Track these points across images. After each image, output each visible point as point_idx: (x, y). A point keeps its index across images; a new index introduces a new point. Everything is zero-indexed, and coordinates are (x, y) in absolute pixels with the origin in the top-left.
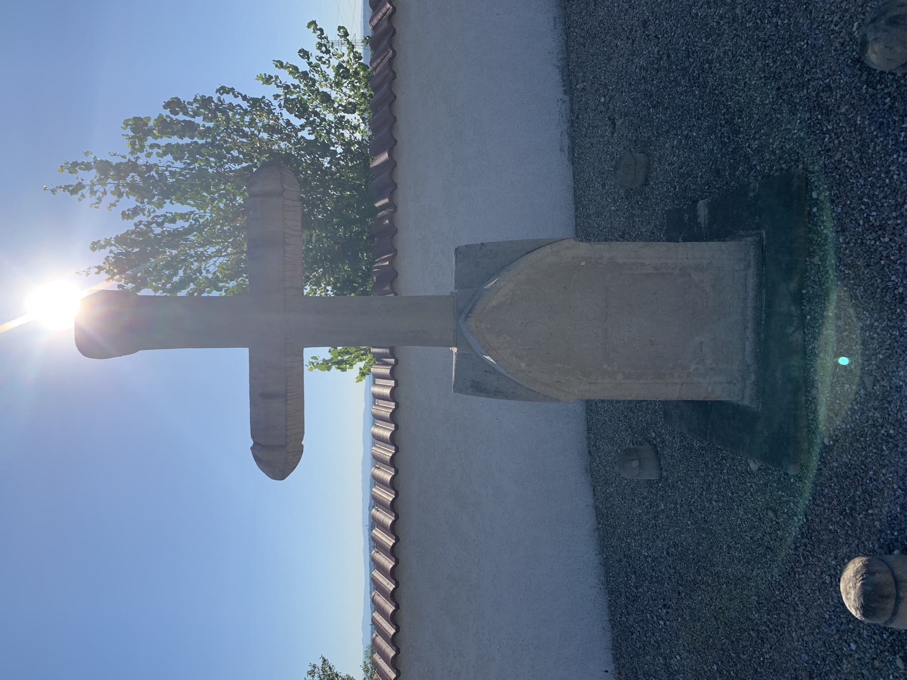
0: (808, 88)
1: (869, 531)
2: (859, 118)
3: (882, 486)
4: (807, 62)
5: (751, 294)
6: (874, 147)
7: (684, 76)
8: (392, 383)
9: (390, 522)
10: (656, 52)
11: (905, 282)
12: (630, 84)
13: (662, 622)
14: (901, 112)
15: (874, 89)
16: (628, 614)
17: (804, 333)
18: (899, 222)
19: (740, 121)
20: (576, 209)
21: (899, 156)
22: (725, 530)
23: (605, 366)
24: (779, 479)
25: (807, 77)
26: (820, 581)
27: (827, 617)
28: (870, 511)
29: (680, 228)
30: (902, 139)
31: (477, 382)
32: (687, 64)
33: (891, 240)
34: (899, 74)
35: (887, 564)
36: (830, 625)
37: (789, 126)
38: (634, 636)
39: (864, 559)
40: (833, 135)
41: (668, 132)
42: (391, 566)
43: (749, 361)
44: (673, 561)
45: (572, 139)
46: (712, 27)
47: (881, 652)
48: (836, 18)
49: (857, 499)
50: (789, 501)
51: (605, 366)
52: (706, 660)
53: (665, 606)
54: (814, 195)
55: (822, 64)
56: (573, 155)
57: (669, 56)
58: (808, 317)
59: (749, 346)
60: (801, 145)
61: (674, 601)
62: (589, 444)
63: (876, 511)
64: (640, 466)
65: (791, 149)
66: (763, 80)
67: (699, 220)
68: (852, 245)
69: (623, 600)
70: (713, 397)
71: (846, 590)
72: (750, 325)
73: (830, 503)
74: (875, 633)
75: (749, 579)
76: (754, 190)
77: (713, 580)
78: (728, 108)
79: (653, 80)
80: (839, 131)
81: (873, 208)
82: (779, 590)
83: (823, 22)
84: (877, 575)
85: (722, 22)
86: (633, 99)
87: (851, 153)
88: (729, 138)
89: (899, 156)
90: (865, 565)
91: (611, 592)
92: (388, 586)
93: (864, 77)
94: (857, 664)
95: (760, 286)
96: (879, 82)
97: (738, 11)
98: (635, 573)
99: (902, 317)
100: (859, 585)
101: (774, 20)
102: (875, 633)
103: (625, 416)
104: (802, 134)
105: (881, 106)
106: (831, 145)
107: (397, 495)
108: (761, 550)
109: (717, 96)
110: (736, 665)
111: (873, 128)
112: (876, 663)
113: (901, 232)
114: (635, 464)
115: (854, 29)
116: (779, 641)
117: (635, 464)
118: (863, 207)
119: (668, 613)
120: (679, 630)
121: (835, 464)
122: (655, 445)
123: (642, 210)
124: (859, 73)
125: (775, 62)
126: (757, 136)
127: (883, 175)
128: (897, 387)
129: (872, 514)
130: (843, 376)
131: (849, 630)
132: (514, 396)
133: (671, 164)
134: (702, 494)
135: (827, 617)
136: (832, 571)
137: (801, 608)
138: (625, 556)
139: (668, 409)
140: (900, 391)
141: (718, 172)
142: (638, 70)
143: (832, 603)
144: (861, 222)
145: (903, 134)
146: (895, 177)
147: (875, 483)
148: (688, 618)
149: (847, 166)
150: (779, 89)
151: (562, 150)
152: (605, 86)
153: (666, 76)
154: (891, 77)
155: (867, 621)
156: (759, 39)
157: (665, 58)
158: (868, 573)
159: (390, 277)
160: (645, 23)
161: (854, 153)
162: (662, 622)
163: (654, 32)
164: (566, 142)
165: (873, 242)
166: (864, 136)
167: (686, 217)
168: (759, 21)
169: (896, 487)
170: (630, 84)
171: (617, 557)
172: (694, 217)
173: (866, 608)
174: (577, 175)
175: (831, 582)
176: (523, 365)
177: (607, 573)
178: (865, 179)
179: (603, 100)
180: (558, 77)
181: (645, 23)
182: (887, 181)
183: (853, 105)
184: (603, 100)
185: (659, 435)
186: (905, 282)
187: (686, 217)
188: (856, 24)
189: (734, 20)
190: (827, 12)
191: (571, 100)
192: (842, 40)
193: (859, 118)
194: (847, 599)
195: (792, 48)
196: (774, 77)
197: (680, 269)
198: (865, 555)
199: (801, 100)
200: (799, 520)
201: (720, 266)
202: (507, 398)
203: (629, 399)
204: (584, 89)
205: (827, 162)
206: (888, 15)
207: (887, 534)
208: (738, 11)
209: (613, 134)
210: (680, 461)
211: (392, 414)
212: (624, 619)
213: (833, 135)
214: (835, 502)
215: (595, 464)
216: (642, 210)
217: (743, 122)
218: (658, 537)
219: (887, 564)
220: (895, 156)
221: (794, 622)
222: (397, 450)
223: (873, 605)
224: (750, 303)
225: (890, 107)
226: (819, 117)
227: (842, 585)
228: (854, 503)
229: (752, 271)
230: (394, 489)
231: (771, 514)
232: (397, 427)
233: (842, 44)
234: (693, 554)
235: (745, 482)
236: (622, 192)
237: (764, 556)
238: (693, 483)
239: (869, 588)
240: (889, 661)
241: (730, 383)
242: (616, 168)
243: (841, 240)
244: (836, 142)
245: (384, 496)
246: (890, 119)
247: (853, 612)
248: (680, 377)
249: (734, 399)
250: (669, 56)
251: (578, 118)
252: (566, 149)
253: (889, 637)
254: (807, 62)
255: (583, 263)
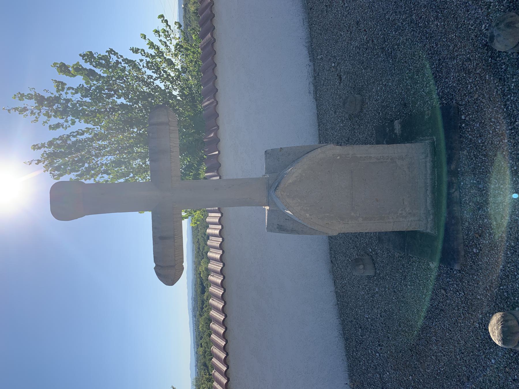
0: (457, 60)
1: (501, 298)
2: (487, 76)
3: (508, 273)
4: (456, 45)
5: (429, 172)
6: (497, 92)
7: (382, 53)
8: (220, 227)
9: (222, 306)
10: (365, 38)
11: (517, 164)
12: (350, 56)
13: (378, 354)
14: (511, 73)
15: (496, 60)
16: (357, 351)
17: (460, 192)
18: (513, 131)
19: (417, 77)
20: (319, 125)
21: (511, 96)
22: (416, 301)
23: (353, 214)
24: (447, 272)
25: (456, 54)
26: (473, 327)
27: (477, 346)
28: (501, 288)
29: (385, 136)
30: (512, 87)
31: (280, 225)
32: (384, 45)
33: (508, 141)
34: (510, 53)
35: (513, 315)
36: (479, 351)
37: (447, 80)
38: (361, 363)
39: (501, 313)
40: (472, 85)
41: (374, 82)
42: (223, 332)
43: (429, 208)
44: (384, 320)
45: (316, 87)
46: (398, 26)
47: (510, 363)
48: (472, 22)
49: (494, 281)
50: (454, 284)
51: (353, 214)
52: (405, 374)
53: (379, 345)
54: (463, 117)
55: (465, 47)
56: (316, 95)
57: (373, 41)
58: (462, 183)
59: (429, 201)
60: (454, 90)
61: (385, 342)
62: (331, 257)
63: (505, 287)
64: (364, 268)
65: (448, 92)
66: (430, 55)
67: (395, 132)
68: (486, 144)
69: (354, 343)
70: (411, 229)
71: (492, 331)
72: (429, 188)
73: (478, 284)
74: (506, 353)
75: (430, 328)
76: (428, 115)
77: (409, 330)
78: (410, 70)
79: (363, 54)
80: (476, 83)
81: (498, 124)
82: (448, 333)
83: (464, 24)
84: (510, 322)
85: (404, 23)
86: (352, 65)
87: (483, 95)
88: (411, 86)
89: (511, 96)
90: (502, 317)
91: (346, 340)
92: (221, 343)
93: (489, 54)
94: (495, 371)
95: (433, 167)
96: (499, 56)
97: (414, 17)
98: (361, 328)
99: (516, 182)
100: (500, 327)
101: (436, 23)
102: (506, 353)
103: (353, 241)
104: (454, 85)
105: (500, 70)
106: (472, 90)
107: (225, 290)
108: (438, 311)
109: (403, 63)
110: (423, 376)
111: (496, 82)
112: (507, 369)
113: (514, 137)
114: (361, 267)
115: (483, 28)
116: (448, 361)
117: (361, 267)
118: (492, 124)
119: (381, 349)
120: (388, 358)
121: (481, 263)
122: (372, 256)
123: (359, 126)
124: (486, 51)
125: (437, 45)
126: (428, 85)
127: (502, 107)
128: (515, 220)
129: (502, 289)
130: (483, 215)
131: (491, 353)
132: (303, 233)
133: (376, 100)
134: (401, 282)
135: (477, 346)
136: (480, 320)
137: (462, 342)
138: (354, 318)
139: (381, 237)
140: (517, 222)
141: (405, 105)
142: (354, 49)
143: (480, 338)
144: (491, 132)
145: (513, 85)
146: (510, 107)
147: (504, 272)
148: (393, 351)
149: (482, 102)
150: (440, 60)
151: (310, 93)
152: (335, 57)
153: (371, 52)
154: (505, 54)
155: (505, 347)
156: (427, 33)
157: (371, 42)
158: (504, 322)
159: (215, 166)
160: (358, 23)
161: (485, 95)
162: (378, 354)
163: (363, 28)
164: (312, 88)
165: (498, 143)
166: (491, 86)
167: (388, 129)
168: (426, 23)
169: (516, 274)
170: (350, 56)
171: (350, 320)
172: (393, 130)
173: (504, 340)
174: (319, 106)
175: (479, 327)
176: (308, 215)
177: (343, 329)
178: (492, 109)
179: (333, 65)
180: (307, 52)
181: (358, 23)
182: (505, 109)
183: (483, 69)
184: (333, 65)
185: (374, 250)
186: (517, 164)
187: (388, 129)
188: (484, 26)
189: (411, 22)
190: (466, 19)
191: (314, 65)
192: (476, 34)
193: (487, 76)
194: (493, 335)
195: (446, 38)
196: (437, 53)
197: (391, 159)
198: (499, 311)
199: (453, 66)
200: (460, 294)
201: (411, 158)
202: (299, 234)
203: (367, 231)
204: (322, 58)
205: (470, 100)
206: (505, 22)
207: (511, 300)
208: (414, 17)
209: (340, 84)
210: (387, 264)
211: (220, 245)
212: (355, 354)
213: (472, 85)
214: (481, 283)
215: (335, 268)
216: (359, 126)
217: (419, 77)
218: (374, 307)
219: (513, 315)
220: (509, 96)
221: (458, 350)
222: (224, 265)
223: (508, 338)
224: (429, 176)
225: (505, 70)
226: (464, 75)
227: (490, 329)
228: (492, 283)
229: (429, 159)
230: (223, 287)
231: (443, 291)
232: (223, 252)
233: (476, 36)
234: (396, 315)
235: (427, 274)
236: (347, 116)
237: (440, 314)
238: (395, 276)
239: (506, 329)
240: (514, 368)
241: (419, 220)
242: (344, 104)
243: (480, 142)
244: (475, 88)
245: (217, 291)
246: (505, 77)
247: (497, 343)
248: (392, 218)
249: (421, 229)
250: (373, 41)
251: (318, 75)
252: (312, 92)
253: (514, 355)
254: (456, 45)
255: (338, 158)
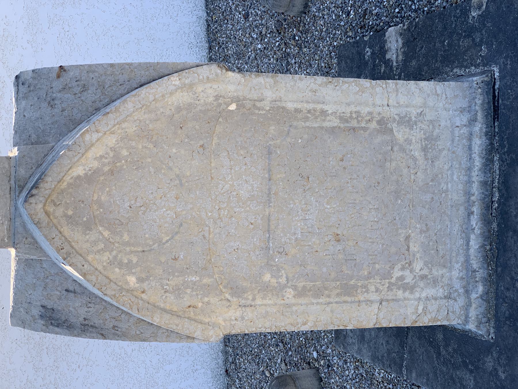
5: (478, 163)
20: (210, 48)
23: (267, 277)
43: (475, 264)
51: (267, 277)
59: (475, 243)
62: (226, 361)
67: (388, 57)
70: (425, 321)
72: (476, 209)
76: (480, 7)
122: (318, 369)
123: (300, 48)
167: (368, 51)
172: (383, 51)
176: (132, 280)
185: (323, 355)
187: (368, 51)
197: (379, 122)
202: (104, 336)
216: (300, 48)
224: (477, 176)
229: (479, 127)
236: (272, 24)
241: (448, 297)
248: (377, 290)
255: (233, 107)
